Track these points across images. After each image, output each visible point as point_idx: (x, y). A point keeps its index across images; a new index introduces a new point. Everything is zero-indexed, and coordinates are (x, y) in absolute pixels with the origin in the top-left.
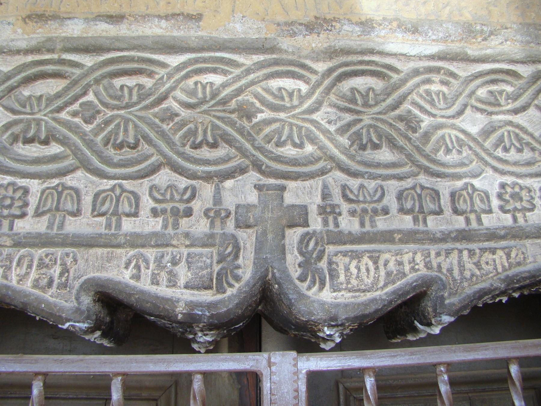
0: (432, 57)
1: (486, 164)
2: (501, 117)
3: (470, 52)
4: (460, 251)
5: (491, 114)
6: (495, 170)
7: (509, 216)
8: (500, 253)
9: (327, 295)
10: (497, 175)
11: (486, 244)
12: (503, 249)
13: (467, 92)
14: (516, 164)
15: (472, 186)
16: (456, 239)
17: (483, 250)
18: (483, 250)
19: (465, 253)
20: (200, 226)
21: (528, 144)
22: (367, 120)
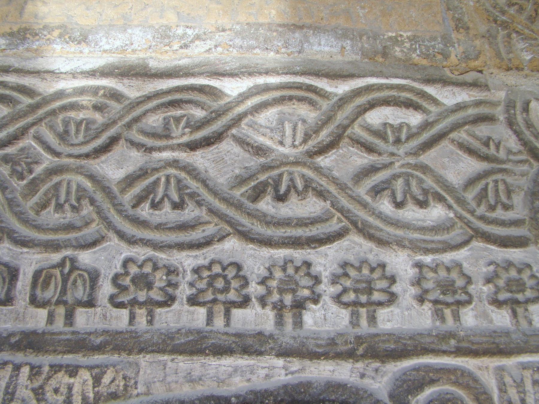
0: (92, 74)
1: (110, 225)
2: (166, 155)
3: (153, 64)
4: (17, 368)
5: (150, 150)
6: (121, 235)
7: (125, 313)
8: (85, 375)
10: (123, 245)
11: (69, 358)
12: (90, 368)
13: (127, 119)
14: (159, 227)
15: (73, 260)
16: (17, 347)
17: (56, 368)
18: (56, 368)
19: (25, 371)
21: (193, 195)
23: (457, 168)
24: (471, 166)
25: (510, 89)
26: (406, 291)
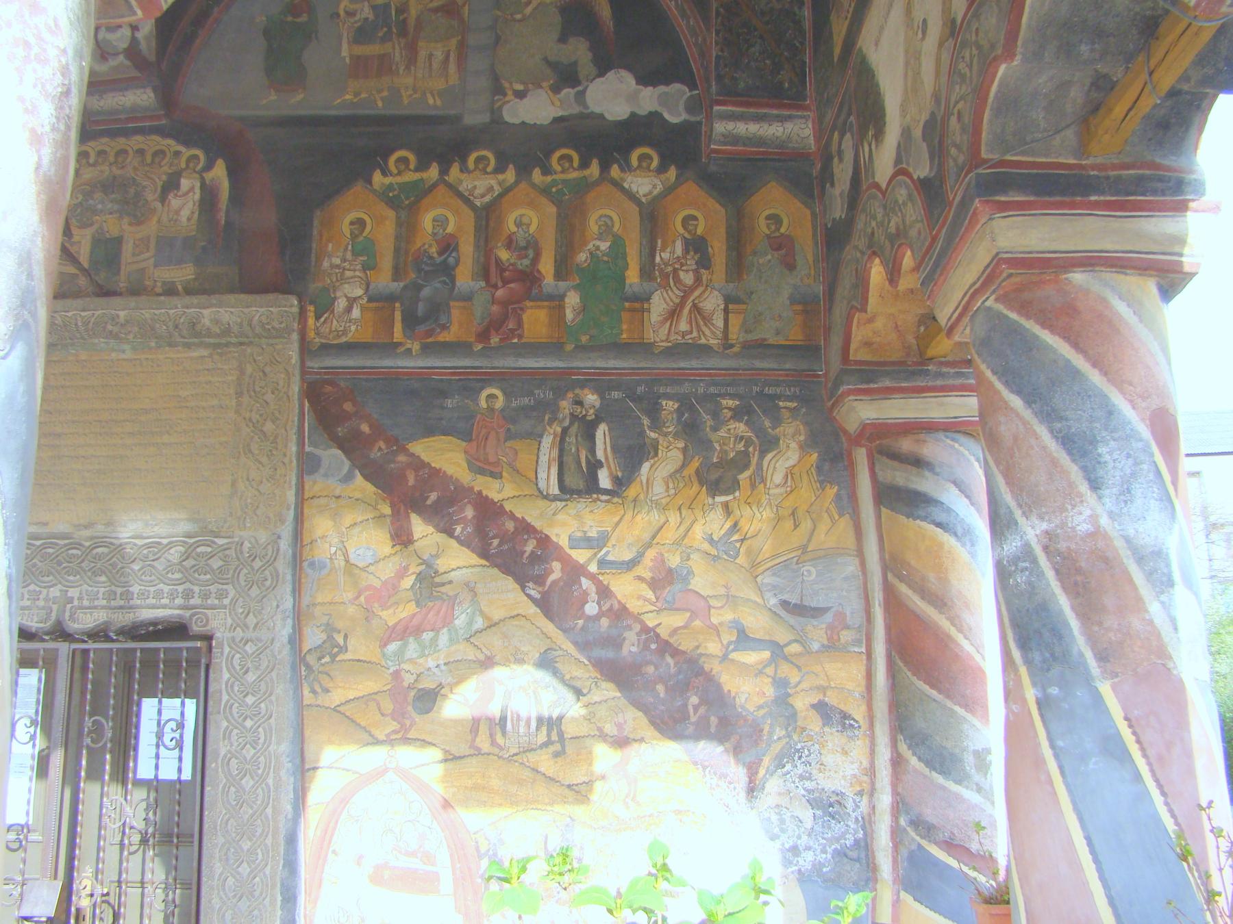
9: (76, 626)
20: (41, 603)
22: (99, 565)
23: (216, 563)
24: (221, 563)
25: (241, 537)
26: (196, 595)
